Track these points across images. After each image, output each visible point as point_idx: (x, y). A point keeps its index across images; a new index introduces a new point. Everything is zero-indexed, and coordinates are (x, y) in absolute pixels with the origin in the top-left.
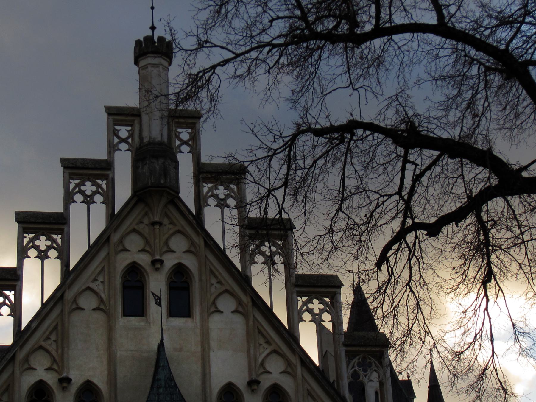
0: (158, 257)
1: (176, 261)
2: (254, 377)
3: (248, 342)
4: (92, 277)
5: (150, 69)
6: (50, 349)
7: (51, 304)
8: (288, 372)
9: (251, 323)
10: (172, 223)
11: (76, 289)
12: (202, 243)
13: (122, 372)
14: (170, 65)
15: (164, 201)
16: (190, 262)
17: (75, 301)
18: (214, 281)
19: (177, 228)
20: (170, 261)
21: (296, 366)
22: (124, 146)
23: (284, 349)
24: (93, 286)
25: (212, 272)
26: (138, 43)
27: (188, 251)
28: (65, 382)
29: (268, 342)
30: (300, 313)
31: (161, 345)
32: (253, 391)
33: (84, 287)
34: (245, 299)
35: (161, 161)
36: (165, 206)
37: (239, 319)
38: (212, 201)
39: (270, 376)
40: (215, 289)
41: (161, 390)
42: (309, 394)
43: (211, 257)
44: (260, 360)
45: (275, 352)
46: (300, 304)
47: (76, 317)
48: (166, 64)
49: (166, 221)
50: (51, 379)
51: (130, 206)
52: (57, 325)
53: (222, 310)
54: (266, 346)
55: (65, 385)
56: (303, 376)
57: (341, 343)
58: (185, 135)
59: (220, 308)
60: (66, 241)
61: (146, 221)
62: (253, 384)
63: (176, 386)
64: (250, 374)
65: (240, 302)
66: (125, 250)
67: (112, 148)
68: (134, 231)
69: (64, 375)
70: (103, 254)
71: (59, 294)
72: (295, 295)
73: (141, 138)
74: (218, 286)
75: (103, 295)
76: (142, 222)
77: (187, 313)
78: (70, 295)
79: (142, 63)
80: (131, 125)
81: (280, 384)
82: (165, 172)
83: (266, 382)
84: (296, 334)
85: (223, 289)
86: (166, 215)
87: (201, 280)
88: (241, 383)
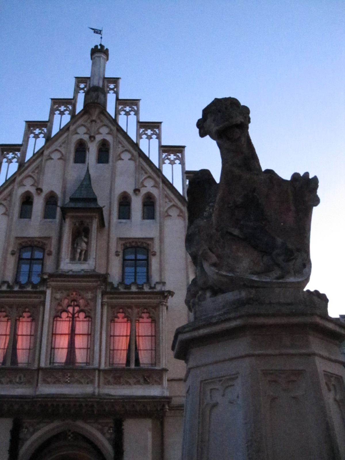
0: (92, 135)
1: (102, 138)
2: (137, 188)
3: (136, 173)
4: (59, 145)
5: (96, 58)
6: (34, 176)
7: (36, 155)
8: (156, 186)
9: (137, 163)
10: (102, 121)
11: (50, 150)
12: (115, 129)
13: (68, 186)
14: (108, 59)
15: (97, 111)
16: (109, 138)
17: (49, 156)
18: (120, 146)
19: (103, 124)
20: (99, 138)
21: (160, 183)
22: (82, 91)
23: (154, 175)
24: (59, 149)
25: (120, 143)
26: (92, 49)
27: (108, 134)
28: (39, 190)
29: (146, 173)
30: (164, 160)
31: (88, 170)
32: (136, 194)
33: (55, 149)
34: (136, 153)
35: (96, 93)
36: (98, 115)
37: (132, 163)
38: (123, 113)
39: (146, 188)
40: (120, 149)
41: (83, 189)
42: (166, 196)
43: (120, 136)
44: (141, 181)
45: (149, 177)
46: (164, 155)
47: (49, 163)
48: (105, 57)
49: (98, 121)
50: (33, 190)
51: (81, 114)
52: (39, 166)
53: (123, 158)
54: (144, 174)
55: (39, 192)
56: (163, 188)
57: (184, 173)
58: (112, 86)
59: (123, 158)
60: (50, 131)
61: (89, 121)
62: (137, 191)
63: (91, 187)
64: (136, 186)
65: (133, 155)
66: (77, 133)
67: (76, 92)
68: (82, 125)
69: (39, 187)
70: (66, 135)
71: (41, 151)
72: (161, 151)
73: (89, 86)
74: (122, 148)
75: (63, 152)
76: (86, 121)
77: (107, 162)
78: (46, 153)
79: (93, 57)
80: (86, 83)
81: (151, 192)
82: (98, 97)
83: (144, 191)
84: (161, 170)
85: (124, 149)
86: (99, 118)
87: (113, 146)
88: (130, 192)
